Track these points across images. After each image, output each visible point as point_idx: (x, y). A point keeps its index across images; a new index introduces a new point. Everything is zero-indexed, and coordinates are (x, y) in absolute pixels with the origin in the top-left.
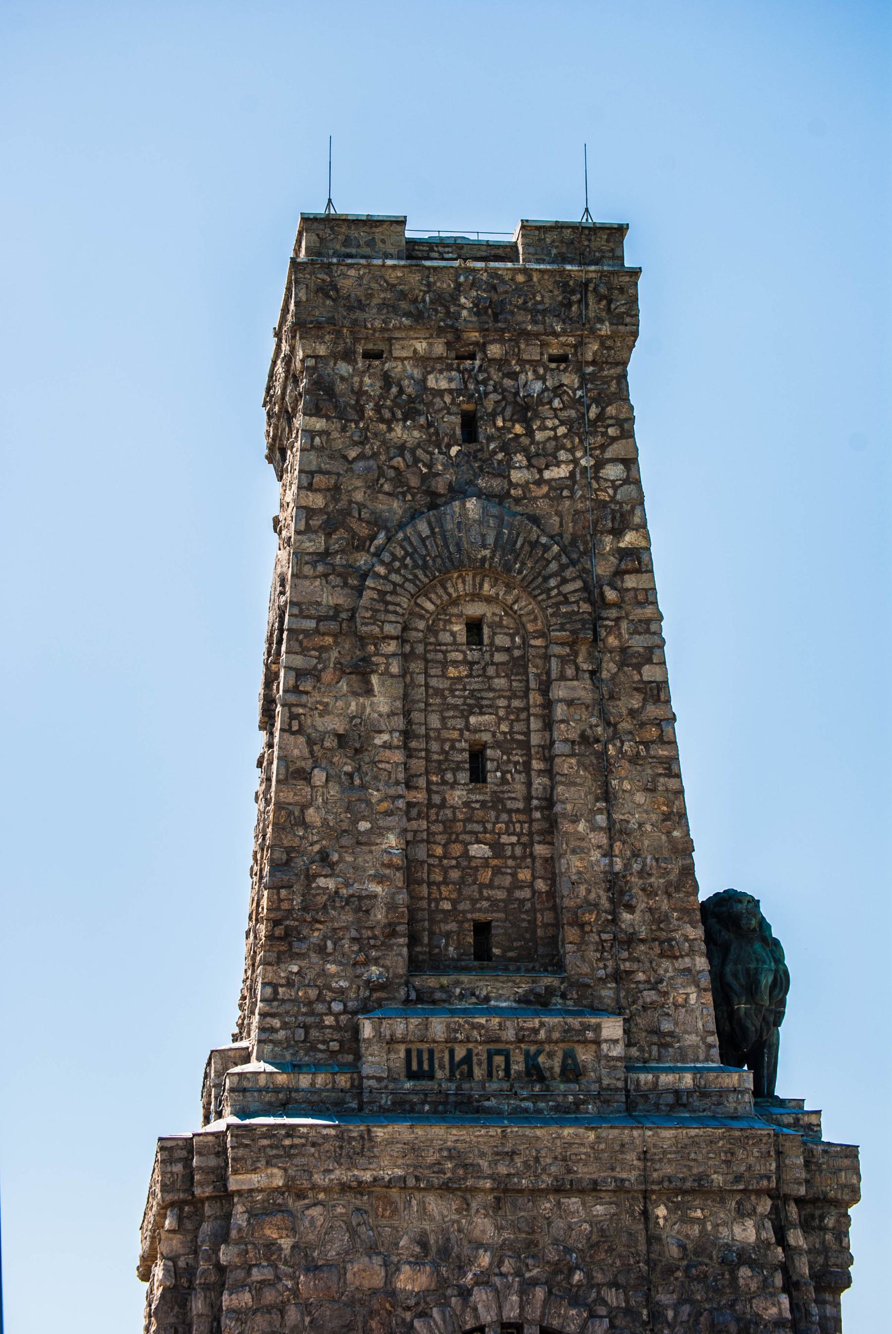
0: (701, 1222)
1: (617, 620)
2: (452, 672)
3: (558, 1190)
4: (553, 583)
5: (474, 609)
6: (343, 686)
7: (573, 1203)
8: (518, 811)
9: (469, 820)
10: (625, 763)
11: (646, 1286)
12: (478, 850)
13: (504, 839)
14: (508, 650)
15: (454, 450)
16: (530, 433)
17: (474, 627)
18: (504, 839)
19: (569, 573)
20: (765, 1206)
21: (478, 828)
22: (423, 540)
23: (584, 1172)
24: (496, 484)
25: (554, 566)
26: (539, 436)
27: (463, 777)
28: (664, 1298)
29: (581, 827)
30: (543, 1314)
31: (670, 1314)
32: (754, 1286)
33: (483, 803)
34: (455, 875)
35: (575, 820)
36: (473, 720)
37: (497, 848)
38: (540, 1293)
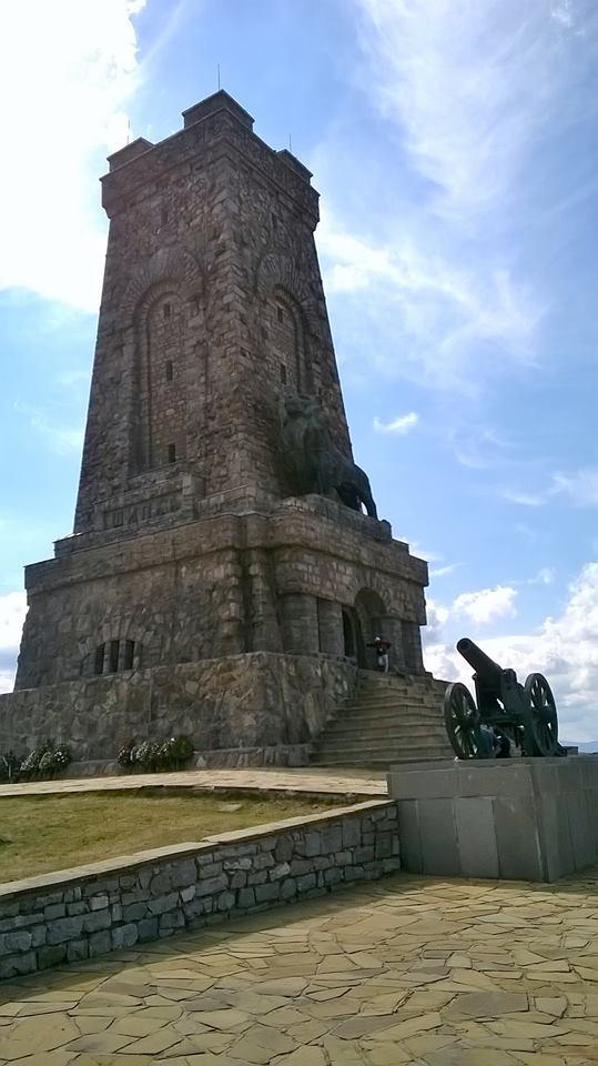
0: (201, 571)
1: (215, 279)
2: (159, 333)
3: (141, 569)
5: (165, 301)
6: (114, 356)
7: (147, 574)
9: (166, 399)
10: (215, 348)
11: (174, 612)
12: (170, 412)
17: (167, 307)
20: (230, 555)
22: (141, 277)
23: (150, 557)
24: (172, 239)
26: (190, 208)
27: (164, 380)
28: (181, 615)
29: (195, 385)
30: (128, 634)
31: (182, 623)
32: (218, 601)
34: (161, 427)
36: (167, 352)
37: (176, 408)
38: (128, 621)
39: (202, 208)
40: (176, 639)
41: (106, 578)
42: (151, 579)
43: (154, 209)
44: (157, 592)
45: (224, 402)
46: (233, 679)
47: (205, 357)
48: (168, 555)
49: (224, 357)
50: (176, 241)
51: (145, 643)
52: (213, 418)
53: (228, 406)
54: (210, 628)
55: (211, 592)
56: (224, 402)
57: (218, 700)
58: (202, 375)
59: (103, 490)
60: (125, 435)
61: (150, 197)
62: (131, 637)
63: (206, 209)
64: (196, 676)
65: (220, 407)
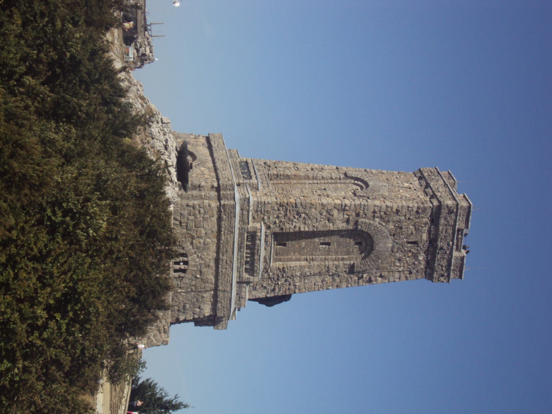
4: (369, 263)
5: (364, 244)
6: (346, 216)
8: (312, 253)
13: (306, 250)
14: (353, 251)
15: (405, 240)
16: (408, 257)
18: (306, 250)
19: (371, 266)
21: (309, 244)
24: (395, 250)
25: (373, 263)
27: (322, 241)
29: (307, 270)
33: (315, 245)
35: (309, 268)
37: (303, 249)
38: (195, 269)
39: (403, 266)
40: (183, 294)
41: (218, 252)
42: (211, 277)
43: (422, 236)
44: (204, 281)
45: (292, 287)
46: (160, 333)
47: (320, 274)
48: (220, 288)
49: (315, 285)
50: (393, 252)
51: (184, 280)
52: (286, 281)
53: (289, 289)
54: (184, 309)
55: (199, 308)
56: (292, 287)
57: (153, 328)
58: (311, 274)
59: (271, 219)
60: (297, 229)
61: (429, 232)
62: (188, 271)
63: (400, 269)
64: (164, 317)
65: (290, 284)
